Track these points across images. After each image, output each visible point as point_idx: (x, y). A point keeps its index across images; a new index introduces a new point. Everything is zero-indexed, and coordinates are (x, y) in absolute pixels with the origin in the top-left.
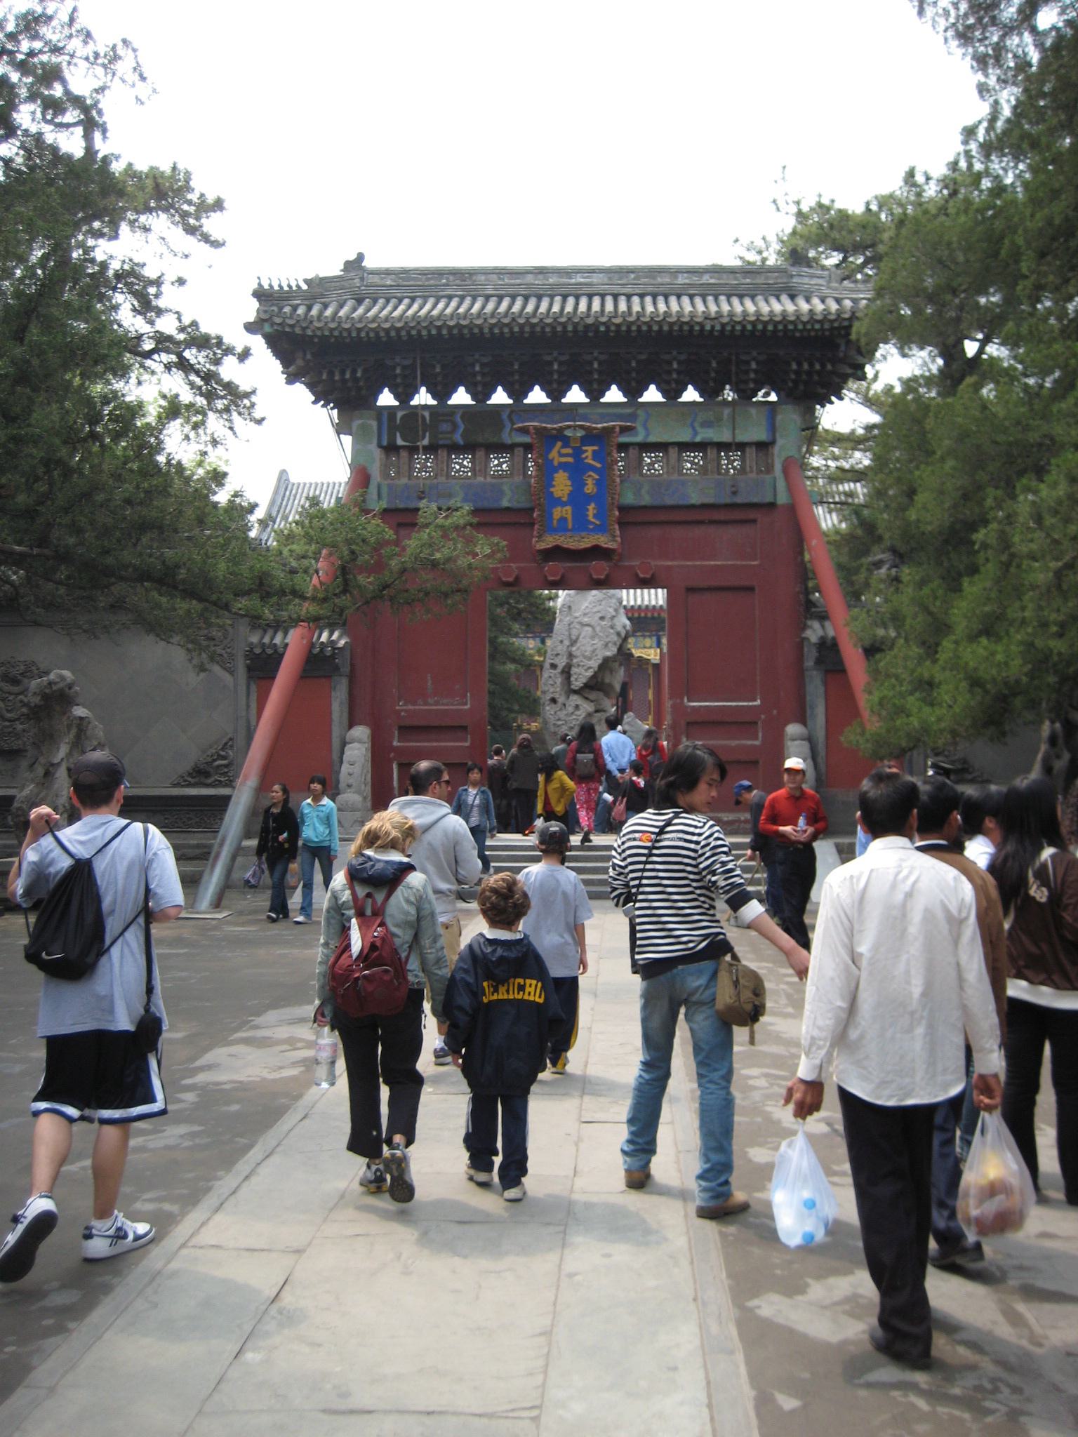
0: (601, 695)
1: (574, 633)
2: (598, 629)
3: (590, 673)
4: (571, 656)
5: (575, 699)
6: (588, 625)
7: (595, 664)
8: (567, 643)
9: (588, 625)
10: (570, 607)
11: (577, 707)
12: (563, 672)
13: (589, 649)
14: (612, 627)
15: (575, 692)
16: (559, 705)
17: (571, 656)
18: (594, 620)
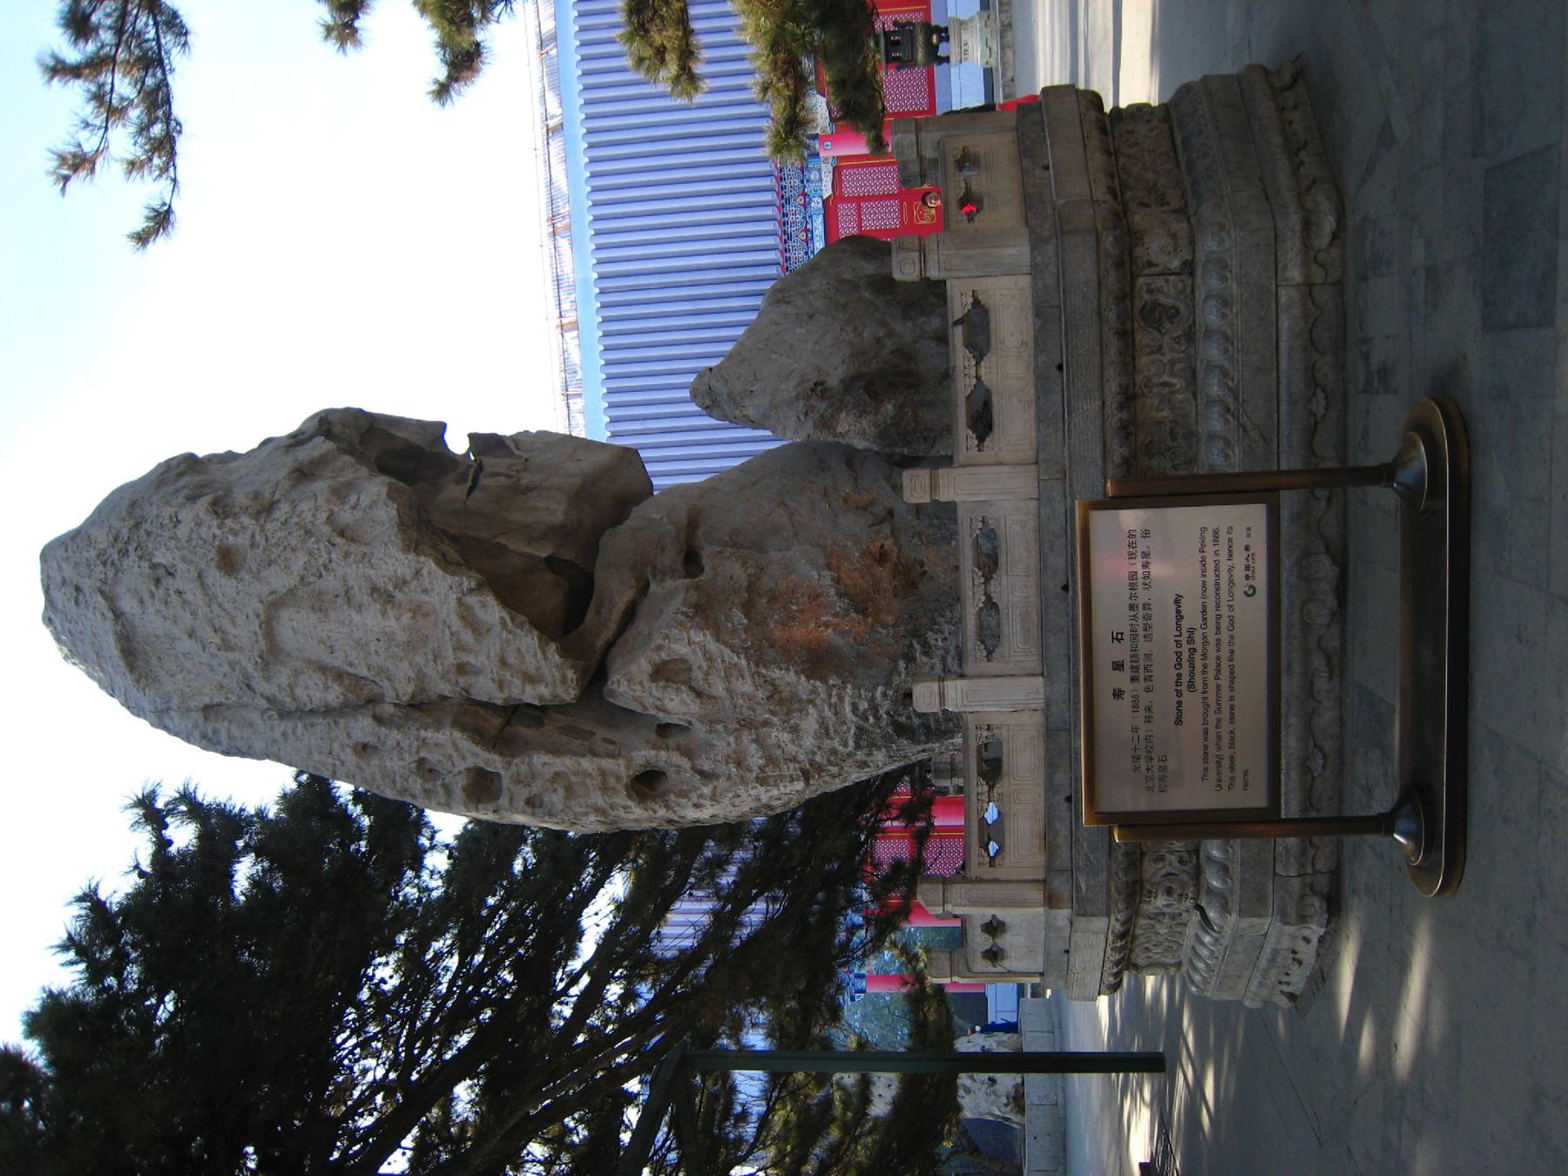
0: (617, 541)
1: (316, 691)
2: (279, 581)
3: (491, 611)
4: (421, 707)
5: (630, 684)
6: (269, 627)
7: (442, 589)
8: (362, 728)
9: (269, 627)
10: (208, 710)
11: (664, 673)
12: (502, 743)
13: (372, 620)
14: (265, 509)
15: (595, 678)
16: (663, 758)
17: (421, 707)
18: (238, 598)
